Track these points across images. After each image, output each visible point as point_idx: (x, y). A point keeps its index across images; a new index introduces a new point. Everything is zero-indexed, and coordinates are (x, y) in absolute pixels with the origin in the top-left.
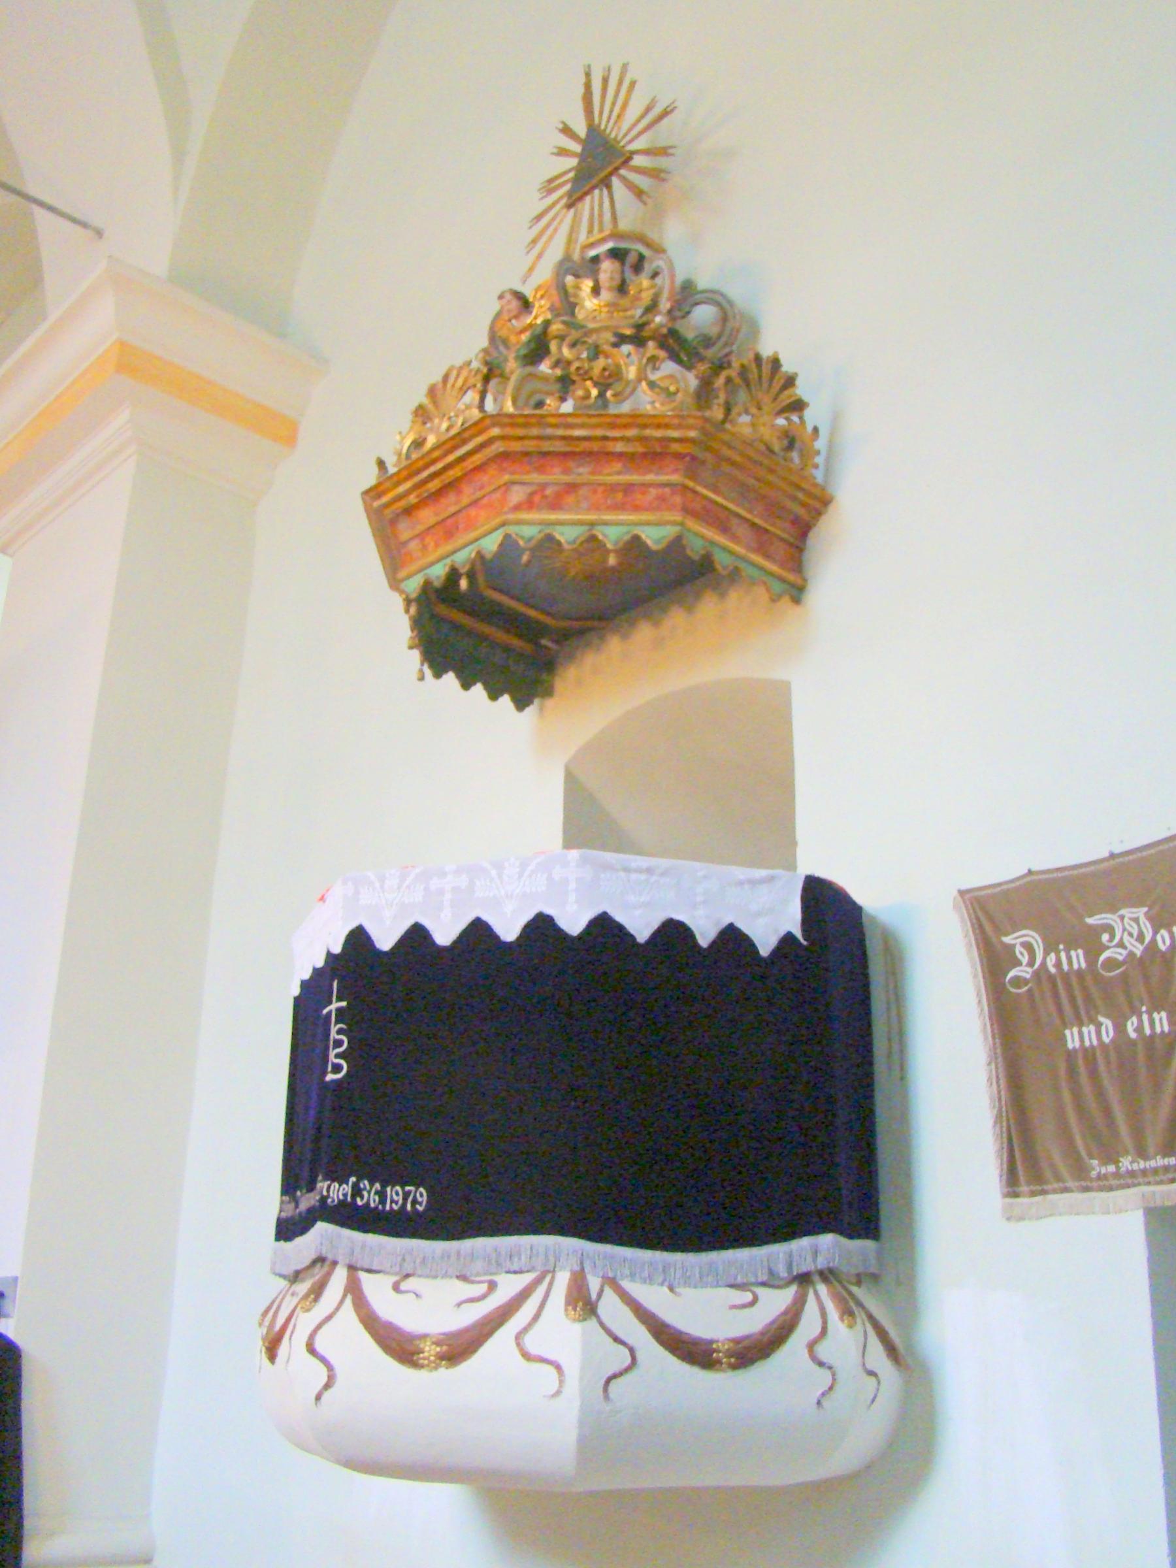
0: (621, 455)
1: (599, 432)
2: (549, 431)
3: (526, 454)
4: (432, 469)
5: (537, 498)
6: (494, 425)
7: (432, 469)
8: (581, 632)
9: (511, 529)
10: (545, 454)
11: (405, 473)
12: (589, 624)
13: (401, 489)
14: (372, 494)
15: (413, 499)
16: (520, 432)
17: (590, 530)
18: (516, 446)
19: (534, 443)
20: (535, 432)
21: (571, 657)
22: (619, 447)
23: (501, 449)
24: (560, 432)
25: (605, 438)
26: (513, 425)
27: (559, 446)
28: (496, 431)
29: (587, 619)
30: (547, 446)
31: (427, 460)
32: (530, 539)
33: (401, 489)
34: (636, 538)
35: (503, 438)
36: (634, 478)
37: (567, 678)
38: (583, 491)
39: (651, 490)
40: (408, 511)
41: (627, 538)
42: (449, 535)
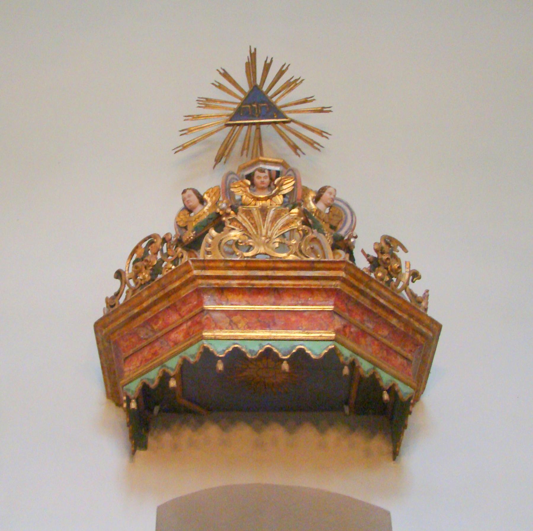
0: (393, 326)
1: (391, 307)
2: (368, 290)
3: (349, 298)
4: (270, 273)
5: (347, 330)
6: (345, 270)
7: (270, 273)
8: (188, 411)
9: (339, 347)
10: (358, 304)
11: (243, 264)
12: (198, 408)
13: (230, 273)
14: (198, 264)
15: (234, 283)
16: (356, 284)
17: (374, 369)
18: (347, 290)
19: (356, 293)
20: (362, 287)
21: (166, 426)
22: (394, 321)
23: (339, 287)
24: (373, 295)
25: (392, 312)
26: (354, 276)
27: (367, 303)
28: (342, 274)
29: (198, 404)
30: (362, 299)
31: (271, 265)
32: (347, 358)
33: (230, 273)
34: (394, 385)
35: (343, 280)
36: (391, 344)
37: (162, 440)
38: (369, 339)
39: (399, 357)
40: (222, 291)
41: (391, 384)
42: (265, 326)
